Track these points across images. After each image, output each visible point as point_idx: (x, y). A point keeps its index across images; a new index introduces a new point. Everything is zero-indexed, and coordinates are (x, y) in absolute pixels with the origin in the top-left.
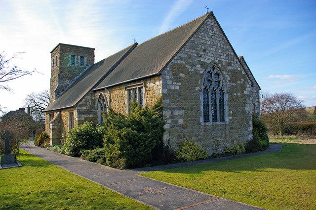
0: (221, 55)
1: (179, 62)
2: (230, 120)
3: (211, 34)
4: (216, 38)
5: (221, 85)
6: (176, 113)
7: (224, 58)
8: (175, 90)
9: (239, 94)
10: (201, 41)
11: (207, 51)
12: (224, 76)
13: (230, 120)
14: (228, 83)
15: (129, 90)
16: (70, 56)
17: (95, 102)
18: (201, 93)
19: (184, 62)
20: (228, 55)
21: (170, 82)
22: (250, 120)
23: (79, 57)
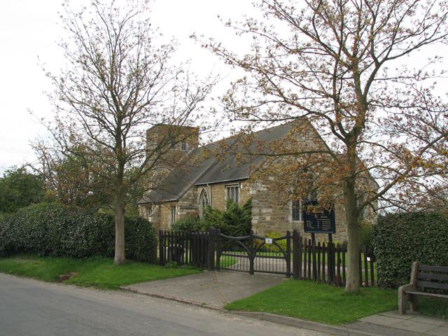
6: (264, 211)
15: (228, 189)
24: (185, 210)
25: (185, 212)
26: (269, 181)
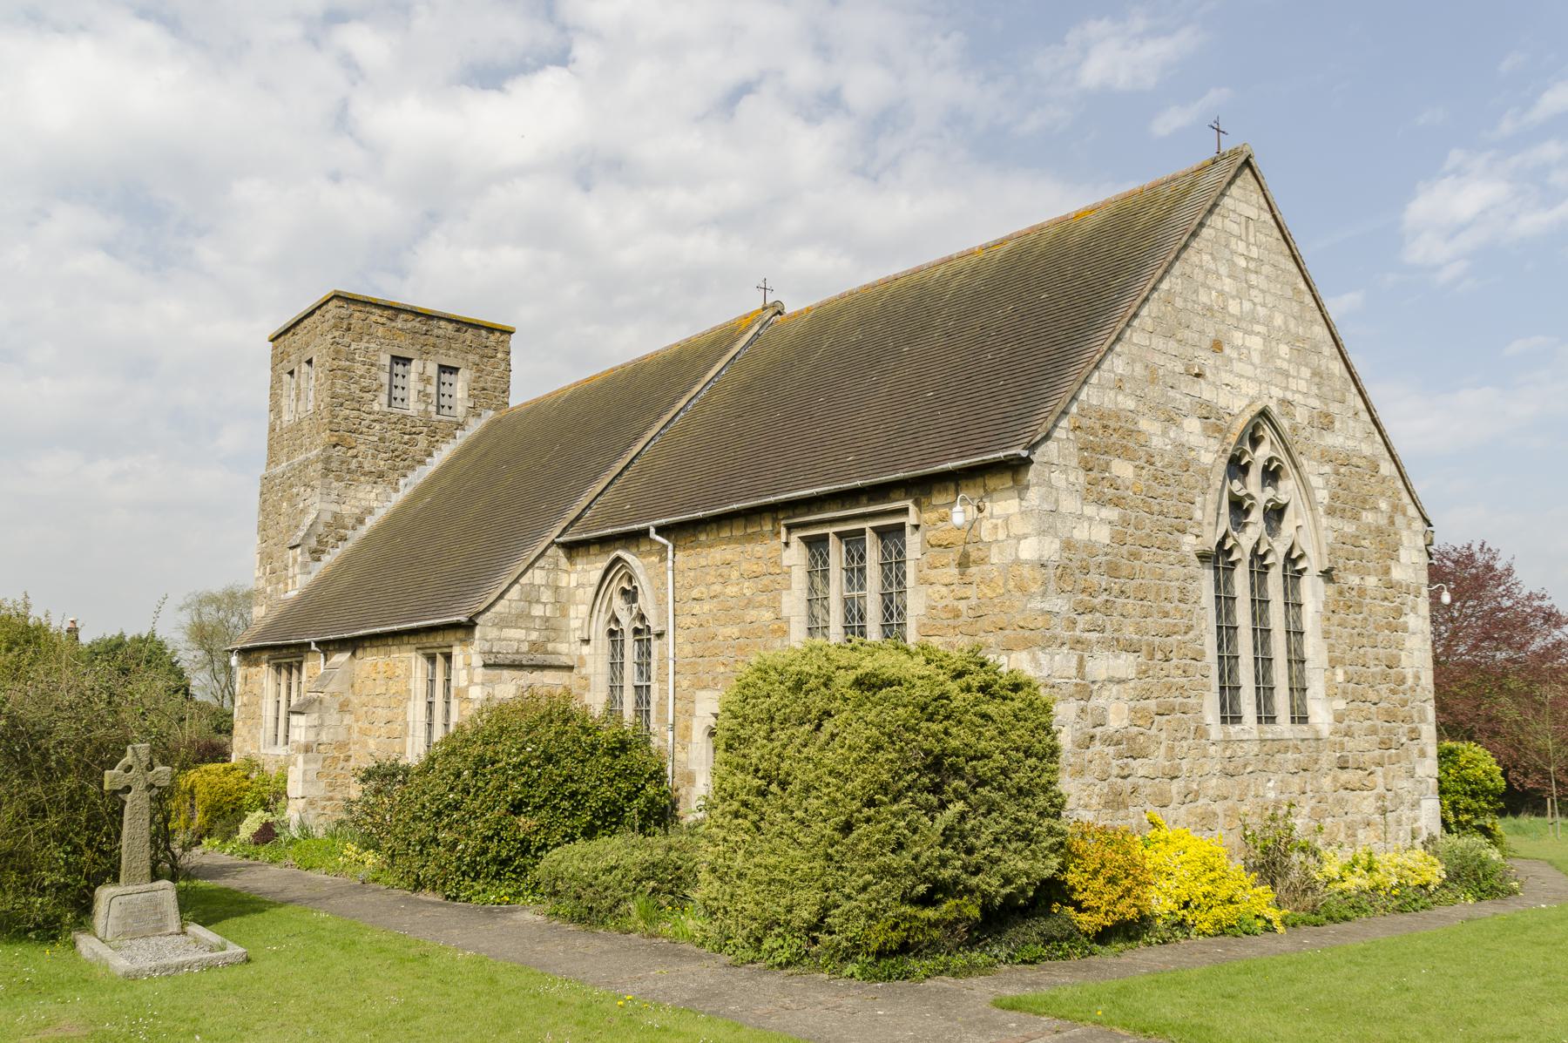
2: (1339, 717)
3: (1243, 263)
4: (1264, 284)
7: (1303, 386)
8: (1090, 546)
9: (1371, 581)
10: (1203, 298)
11: (1227, 350)
12: (1303, 481)
14: (1325, 521)
16: (385, 360)
17: (571, 599)
20: (1316, 373)
23: (432, 369)
24: (506, 673)
25: (508, 687)
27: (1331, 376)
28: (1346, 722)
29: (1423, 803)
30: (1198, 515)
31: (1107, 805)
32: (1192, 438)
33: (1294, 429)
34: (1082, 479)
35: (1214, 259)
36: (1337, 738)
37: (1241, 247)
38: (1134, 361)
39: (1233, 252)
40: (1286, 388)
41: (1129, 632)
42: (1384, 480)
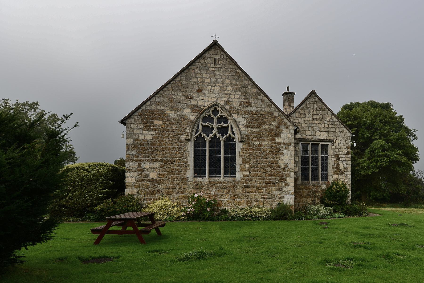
0: (230, 95)
1: (154, 108)
5: (230, 132)
6: (146, 165)
7: (237, 96)
8: (144, 140)
10: (194, 80)
11: (203, 91)
13: (245, 176)
18: (190, 142)
19: (163, 108)
21: (136, 132)
22: (289, 176)
26: (155, 126)
27: (251, 92)
28: (250, 177)
29: (285, 197)
30: (187, 131)
31: (147, 194)
32: (186, 113)
33: (232, 107)
34: (142, 126)
35: (200, 70)
36: (244, 181)
37: (213, 65)
38: (164, 98)
39: (208, 67)
40: (230, 98)
41: (158, 158)
42: (275, 117)
